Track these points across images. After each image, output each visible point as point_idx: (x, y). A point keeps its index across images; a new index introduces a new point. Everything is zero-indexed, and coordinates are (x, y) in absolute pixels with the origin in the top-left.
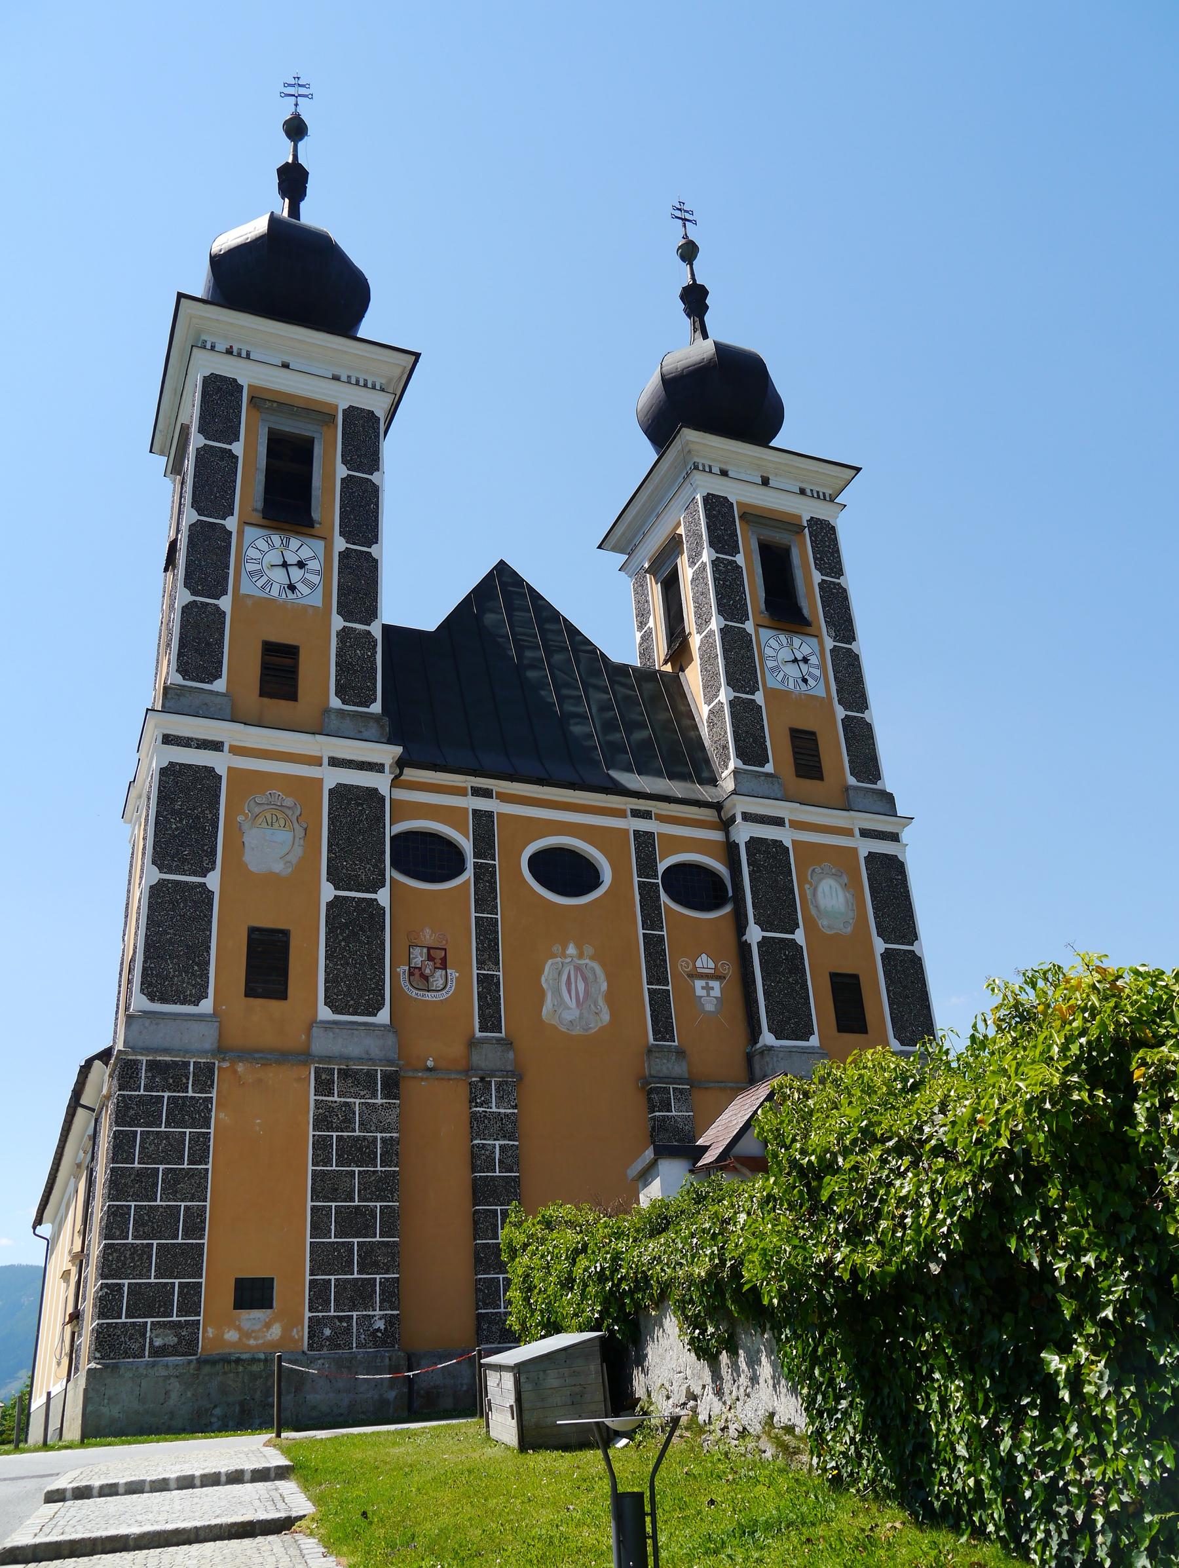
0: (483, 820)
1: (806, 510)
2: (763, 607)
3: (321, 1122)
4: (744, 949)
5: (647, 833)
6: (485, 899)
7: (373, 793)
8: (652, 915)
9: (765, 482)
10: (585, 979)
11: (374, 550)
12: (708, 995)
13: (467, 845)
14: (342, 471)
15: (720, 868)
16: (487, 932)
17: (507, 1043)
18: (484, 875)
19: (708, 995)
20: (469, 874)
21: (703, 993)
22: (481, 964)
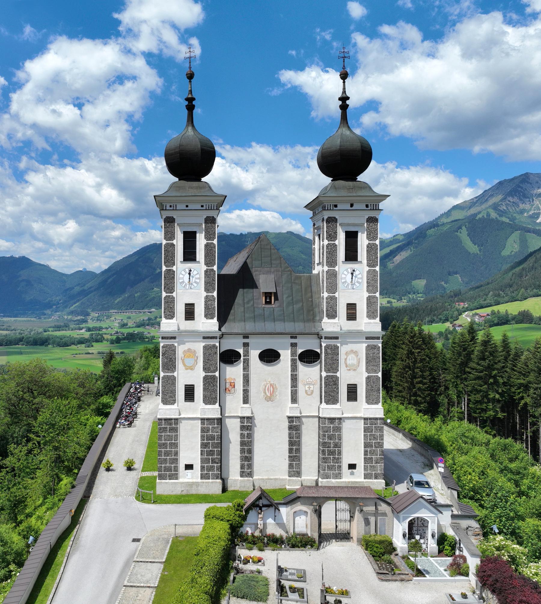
3: (203, 430)
4: (321, 376)
5: (294, 343)
6: (246, 368)
7: (214, 346)
8: (294, 368)
9: (352, 205)
10: (273, 387)
12: (309, 389)
15: (318, 351)
19: (309, 389)
21: (308, 389)
22: (244, 386)
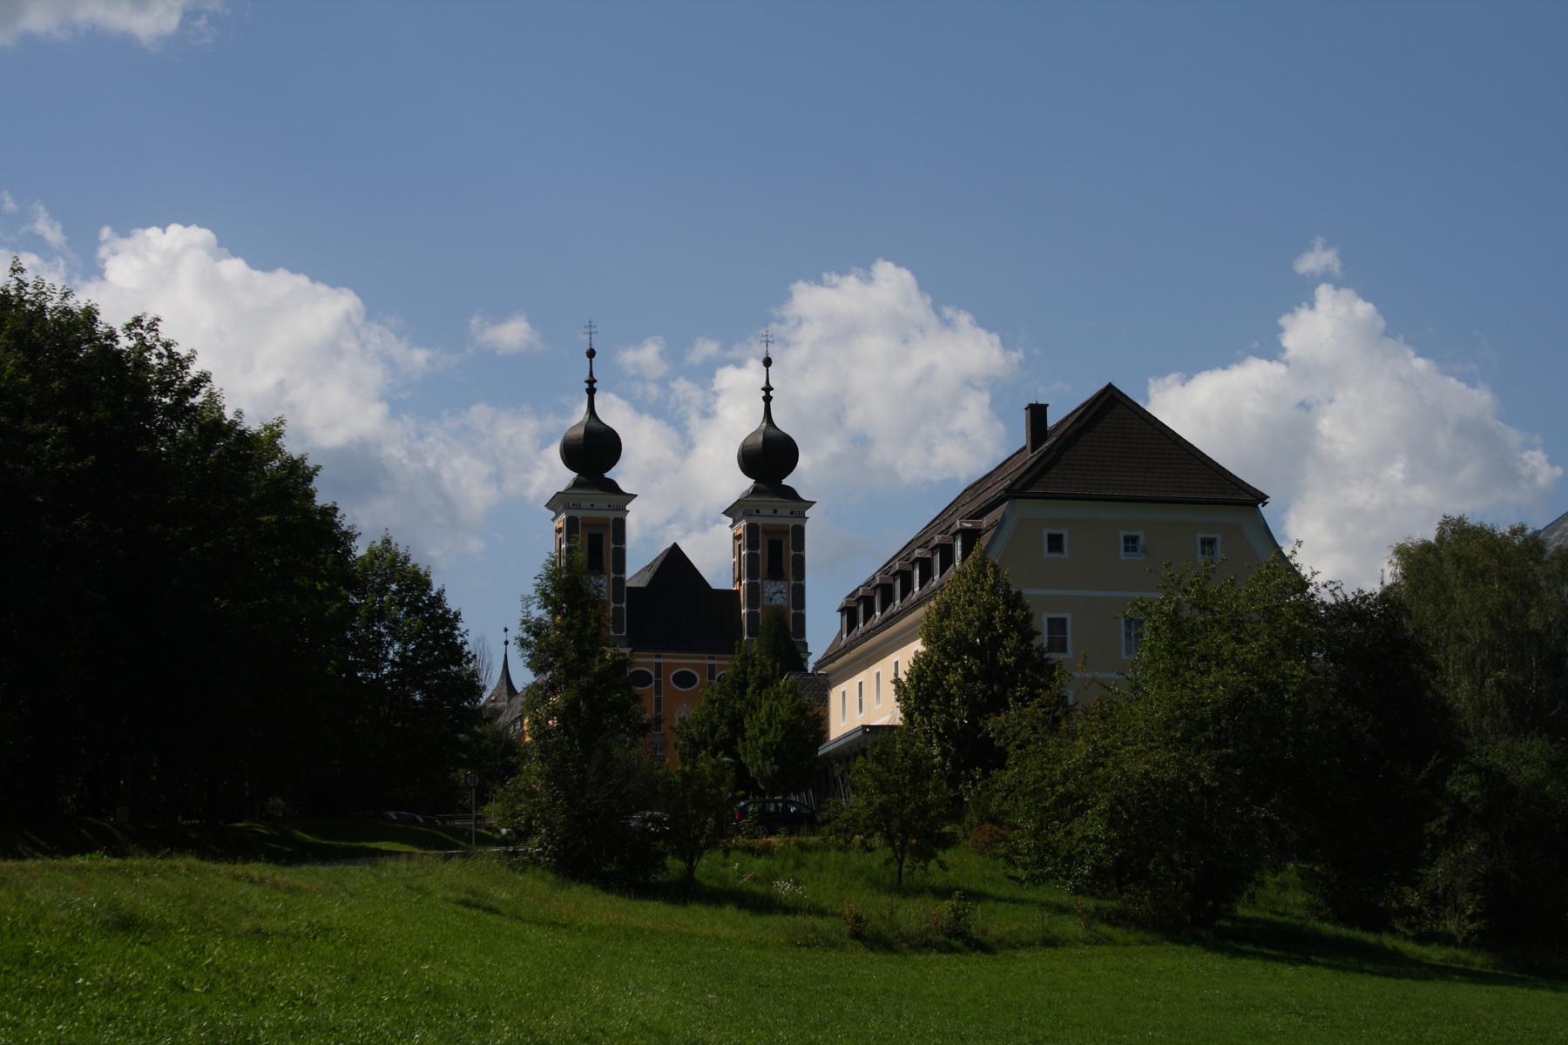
0: (658, 665)
1: (791, 522)
2: (766, 570)
6: (658, 691)
9: (775, 511)
11: (623, 576)
13: (653, 674)
14: (612, 546)
16: (658, 701)
17: (663, 735)
18: (658, 684)
20: (654, 683)
